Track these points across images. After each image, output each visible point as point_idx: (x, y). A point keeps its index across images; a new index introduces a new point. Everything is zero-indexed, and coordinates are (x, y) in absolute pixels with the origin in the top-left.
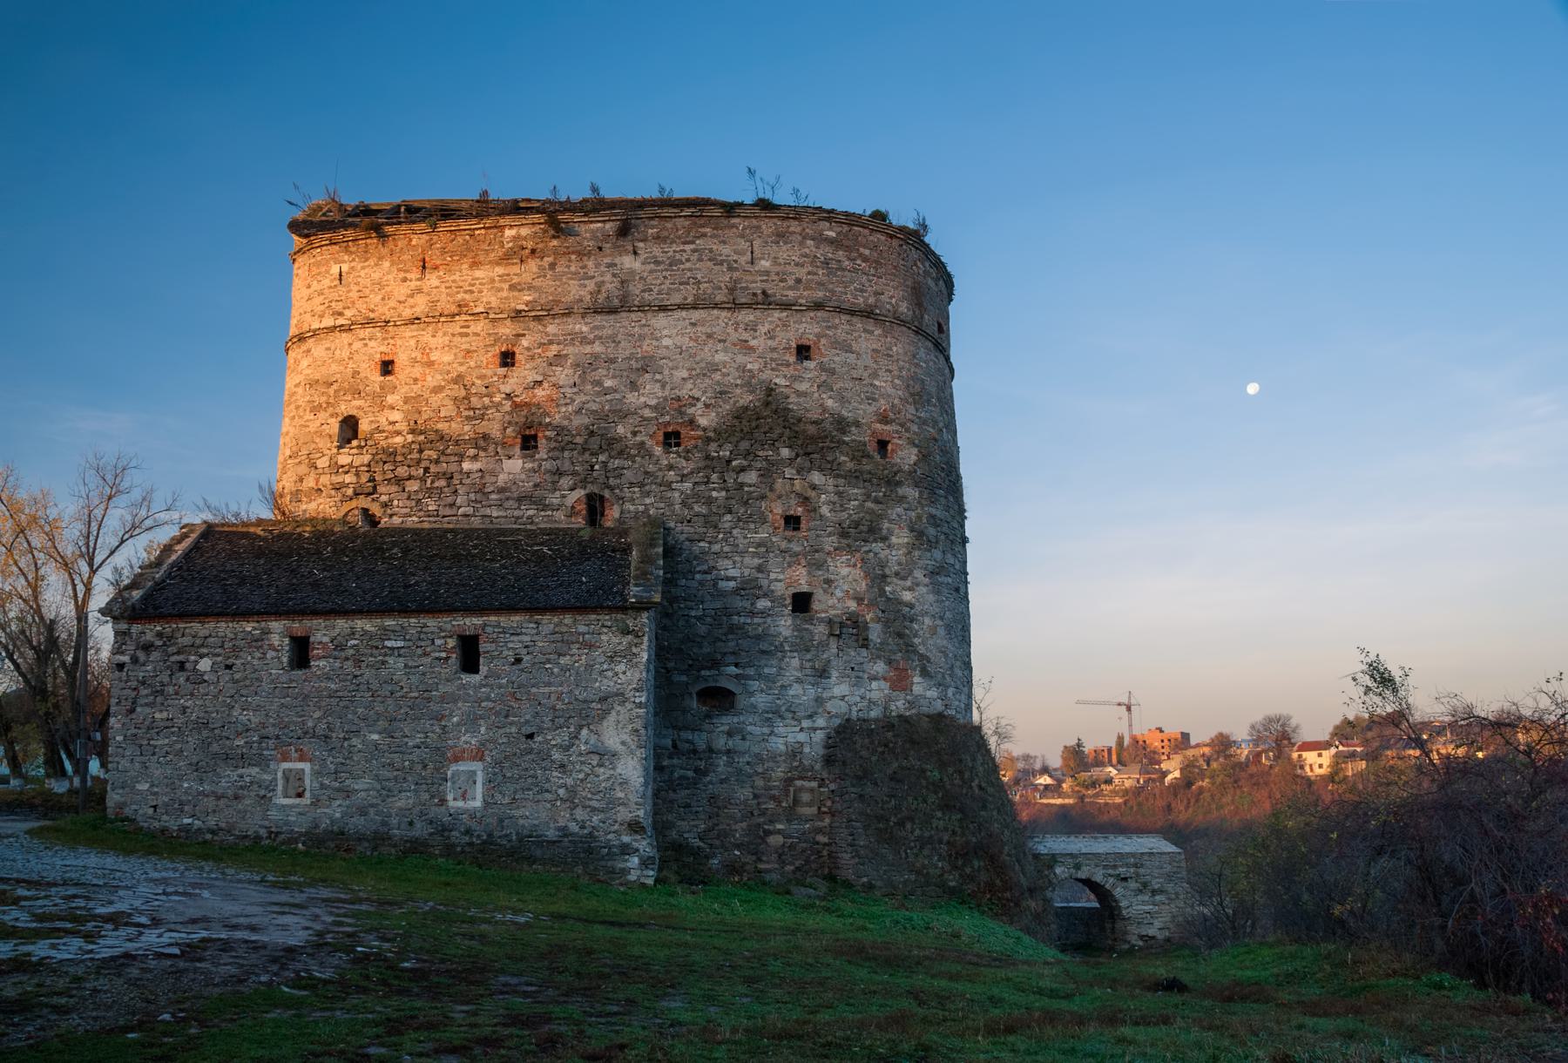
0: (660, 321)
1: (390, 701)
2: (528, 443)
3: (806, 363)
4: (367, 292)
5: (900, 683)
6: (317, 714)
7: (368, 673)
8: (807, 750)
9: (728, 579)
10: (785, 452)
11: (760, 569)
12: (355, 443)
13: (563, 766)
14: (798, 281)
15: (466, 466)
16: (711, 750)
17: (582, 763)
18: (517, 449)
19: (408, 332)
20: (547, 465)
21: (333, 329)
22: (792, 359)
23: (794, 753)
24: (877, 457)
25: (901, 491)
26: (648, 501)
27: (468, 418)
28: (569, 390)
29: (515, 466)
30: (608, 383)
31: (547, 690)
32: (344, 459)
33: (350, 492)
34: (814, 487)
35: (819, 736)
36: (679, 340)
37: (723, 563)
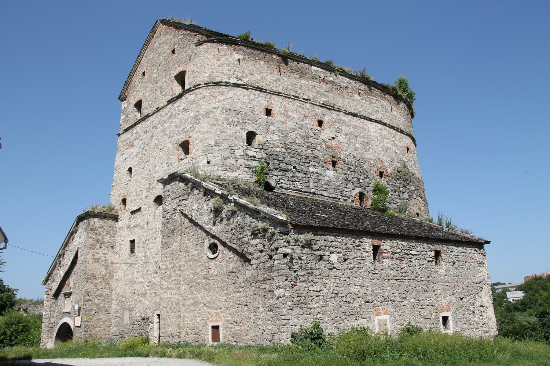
1: (416, 282)
2: (334, 164)
6: (389, 288)
18: (331, 166)
19: (277, 98)
29: (330, 173)
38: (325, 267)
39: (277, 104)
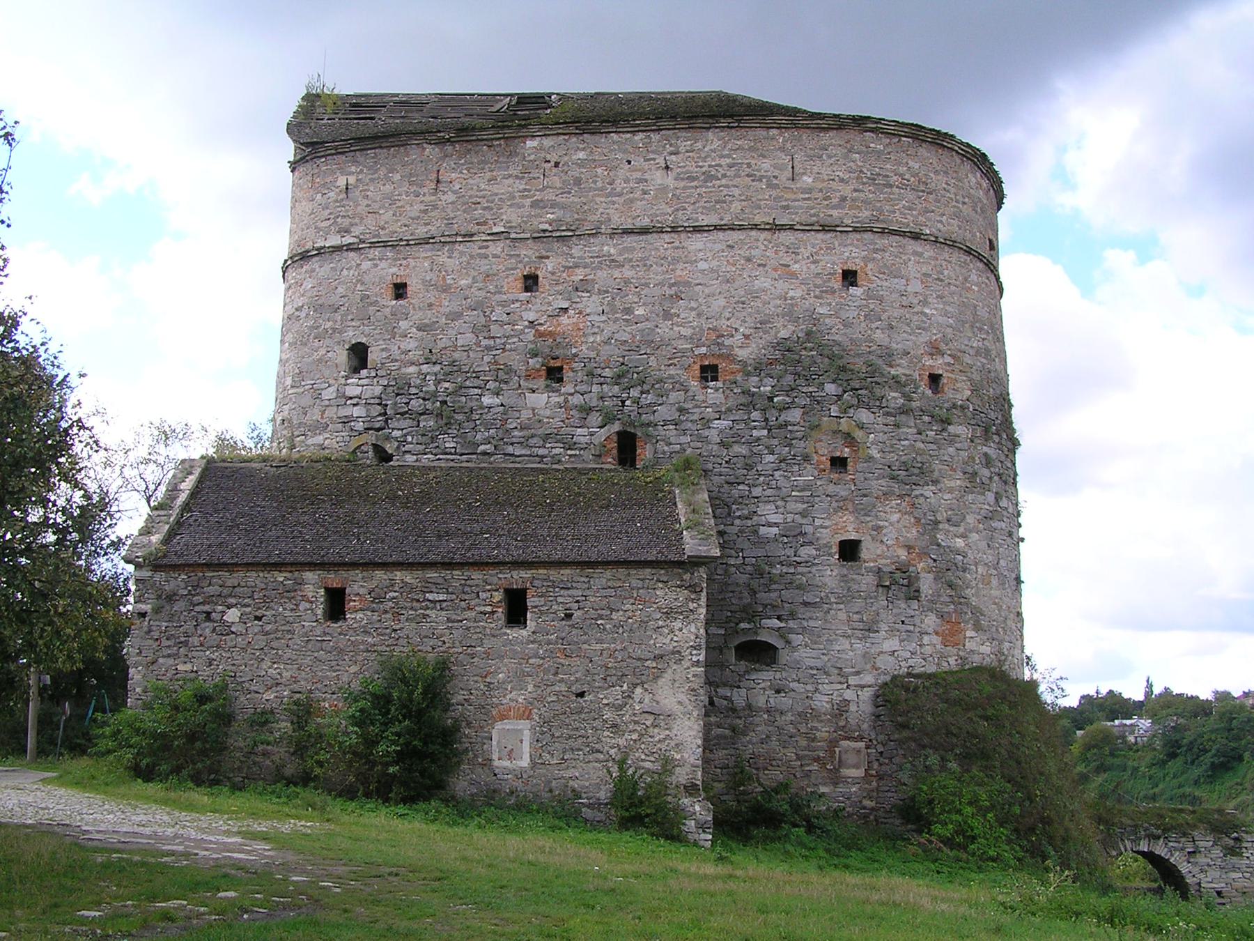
0: (696, 243)
2: (554, 374)
3: (852, 290)
4: (375, 206)
5: (951, 636)
6: (354, 669)
7: (409, 628)
8: (853, 708)
9: (770, 525)
10: (831, 388)
11: (804, 514)
12: (364, 372)
13: (615, 726)
14: (844, 199)
15: (487, 400)
16: (749, 706)
17: (636, 722)
19: (423, 252)
20: (576, 400)
21: (337, 249)
22: (837, 284)
23: (841, 709)
24: (929, 392)
25: (951, 429)
26: (684, 439)
27: (488, 348)
28: (597, 318)
29: (540, 401)
30: (640, 312)
31: (598, 647)
32: (352, 391)
33: (360, 426)
34: (861, 426)
35: (867, 694)
36: (715, 263)
37: (764, 509)
38: (214, 630)
39: (418, 269)
